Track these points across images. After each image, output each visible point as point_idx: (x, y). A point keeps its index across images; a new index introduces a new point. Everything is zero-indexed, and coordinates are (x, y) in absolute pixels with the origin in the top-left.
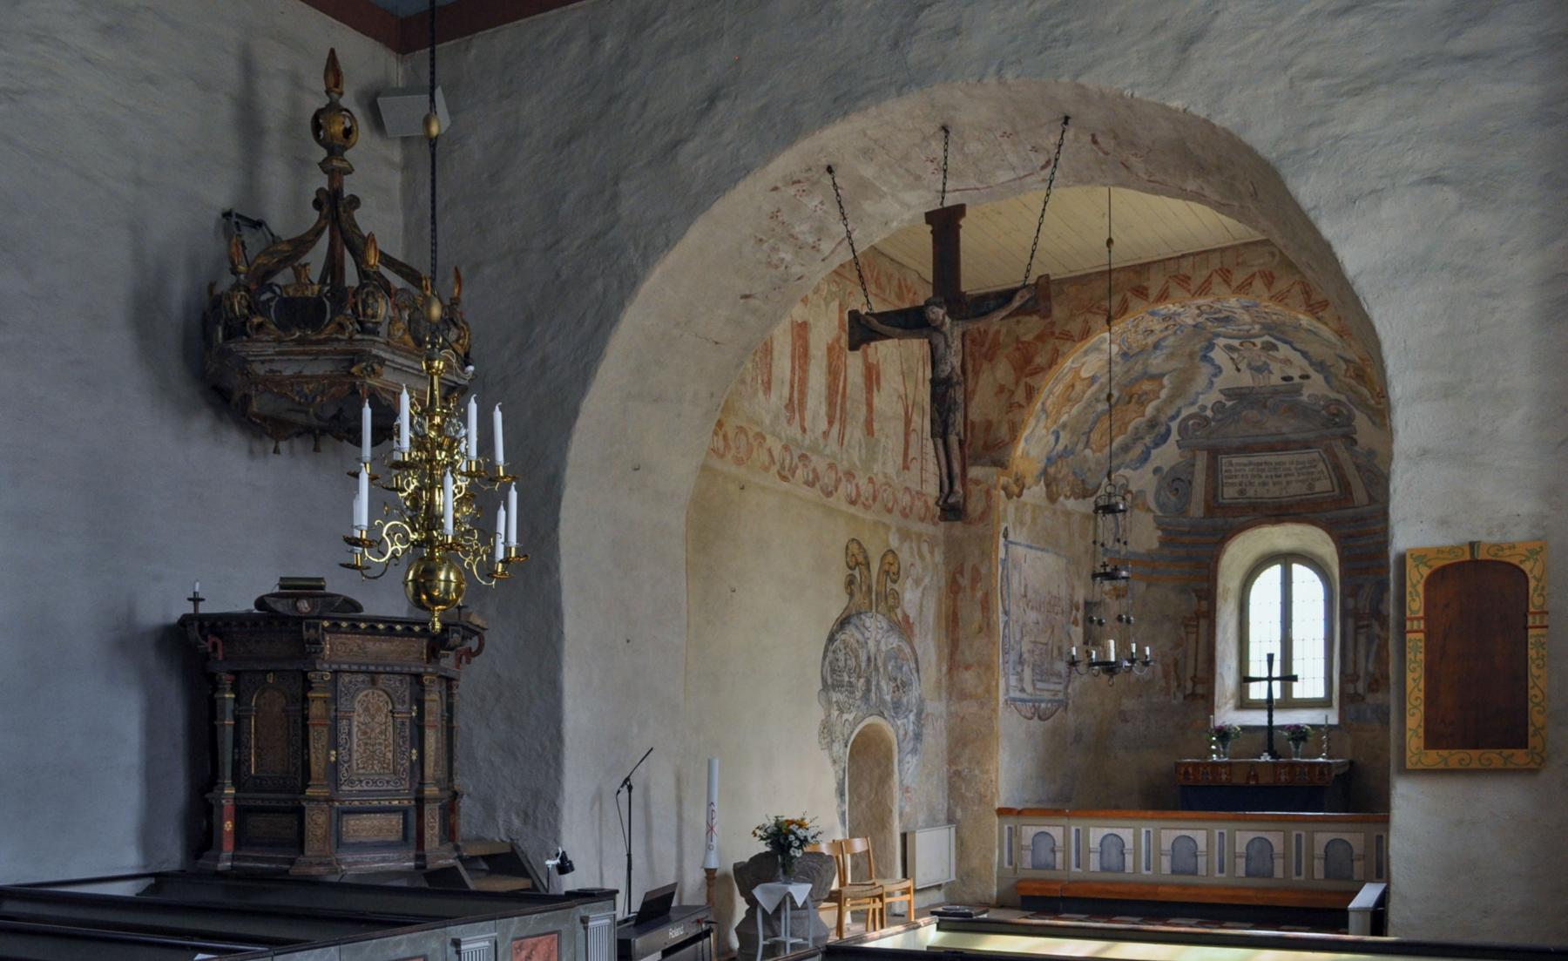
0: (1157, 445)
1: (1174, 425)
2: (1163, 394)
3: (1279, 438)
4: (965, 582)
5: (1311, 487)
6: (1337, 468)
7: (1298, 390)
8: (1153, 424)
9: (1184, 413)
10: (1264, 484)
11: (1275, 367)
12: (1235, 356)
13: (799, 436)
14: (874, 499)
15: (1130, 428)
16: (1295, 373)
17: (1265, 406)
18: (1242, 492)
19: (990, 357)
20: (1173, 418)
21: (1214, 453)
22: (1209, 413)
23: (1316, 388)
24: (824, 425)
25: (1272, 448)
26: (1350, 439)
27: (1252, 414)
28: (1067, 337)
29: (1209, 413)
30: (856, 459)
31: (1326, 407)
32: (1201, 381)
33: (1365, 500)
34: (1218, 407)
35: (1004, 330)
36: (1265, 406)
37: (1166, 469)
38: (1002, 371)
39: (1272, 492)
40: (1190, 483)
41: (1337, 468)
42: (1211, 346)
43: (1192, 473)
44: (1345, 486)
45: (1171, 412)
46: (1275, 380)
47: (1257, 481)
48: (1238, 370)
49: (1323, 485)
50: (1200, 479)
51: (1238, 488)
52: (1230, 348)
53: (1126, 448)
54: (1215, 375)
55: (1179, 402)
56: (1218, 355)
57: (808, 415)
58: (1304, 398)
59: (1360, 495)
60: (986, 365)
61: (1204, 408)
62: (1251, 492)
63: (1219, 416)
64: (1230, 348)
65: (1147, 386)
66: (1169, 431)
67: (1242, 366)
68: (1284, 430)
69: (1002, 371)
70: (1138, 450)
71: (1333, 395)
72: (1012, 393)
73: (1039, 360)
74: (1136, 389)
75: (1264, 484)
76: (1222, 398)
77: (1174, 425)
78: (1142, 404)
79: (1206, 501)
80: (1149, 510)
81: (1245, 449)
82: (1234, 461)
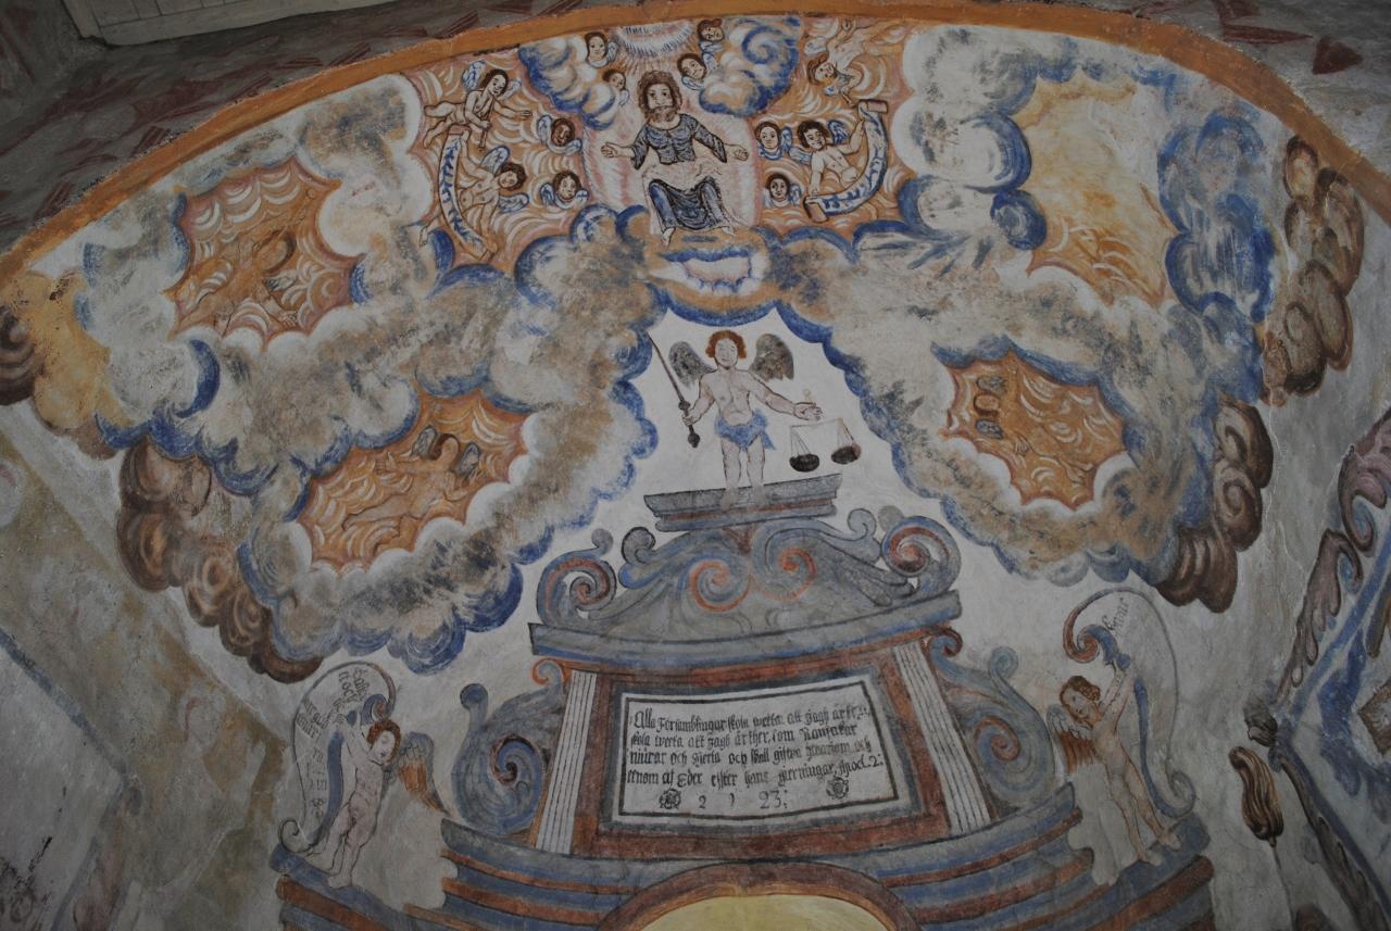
0: (482, 623)
1: (531, 574)
2: (520, 469)
3: (768, 646)
5: (838, 787)
6: (905, 731)
7: (823, 501)
8: (481, 555)
9: (561, 546)
10: (725, 779)
11: (779, 426)
12: (691, 393)
15: (427, 534)
16: (823, 444)
17: (744, 548)
18: (670, 800)
20: (531, 553)
21: (615, 681)
22: (614, 558)
23: (871, 490)
25: (748, 678)
26: (942, 638)
27: (714, 571)
29: (614, 558)
31: (892, 543)
32: (602, 467)
33: (981, 815)
34: (638, 544)
36: (744, 548)
37: (494, 703)
39: (739, 803)
40: (548, 758)
41: (905, 731)
42: (639, 355)
43: (555, 732)
44: (924, 781)
45: (529, 534)
46: (778, 469)
47: (707, 771)
48: (694, 439)
49: (870, 783)
50: (571, 752)
51: (659, 788)
52: (685, 364)
53: (405, 595)
54: (640, 452)
55: (551, 512)
56: (653, 384)
58: (838, 523)
59: (965, 803)
61: (603, 541)
62: (690, 800)
63: (636, 574)
64: (685, 364)
65: (482, 427)
66: (516, 588)
67: (705, 428)
68: (785, 619)
70: (430, 618)
71: (911, 505)
74: (454, 420)
75: (725, 779)
76: (650, 521)
77: (531, 574)
78: (467, 478)
79: (579, 815)
80: (434, 800)
81: (691, 681)
82: (659, 711)
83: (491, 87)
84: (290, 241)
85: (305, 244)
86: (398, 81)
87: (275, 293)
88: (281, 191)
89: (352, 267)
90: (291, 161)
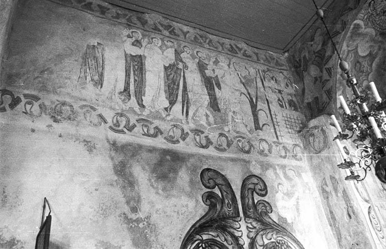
4: (329, 188)
13: (137, 108)
14: (229, 145)
19: (306, 70)
24: (166, 104)
28: (338, 33)
30: (203, 122)
35: (307, 55)
38: (313, 71)
57: (147, 99)
60: (305, 74)
69: (313, 71)
72: (321, 77)
73: (328, 53)
83: (372, 5)
84: (358, 62)
85: (360, 60)
86: (355, 22)
87: (363, 72)
88: (351, 57)
89: (370, 54)
90: (349, 51)
